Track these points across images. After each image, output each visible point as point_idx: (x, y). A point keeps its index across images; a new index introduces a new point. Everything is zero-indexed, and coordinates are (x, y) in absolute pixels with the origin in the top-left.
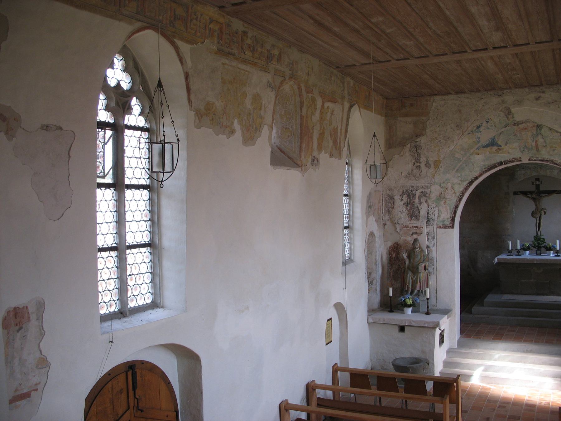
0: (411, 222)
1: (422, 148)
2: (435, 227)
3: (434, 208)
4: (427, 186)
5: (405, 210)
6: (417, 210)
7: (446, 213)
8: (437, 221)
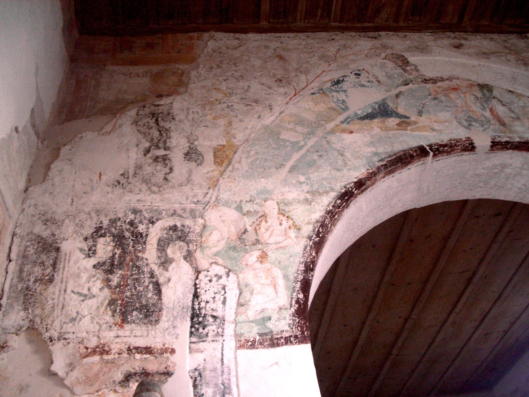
0: (121, 333)
1: (177, 118)
2: (230, 344)
3: (220, 277)
4: (192, 211)
5: (101, 289)
6: (151, 287)
7: (270, 290)
8: (236, 323)
